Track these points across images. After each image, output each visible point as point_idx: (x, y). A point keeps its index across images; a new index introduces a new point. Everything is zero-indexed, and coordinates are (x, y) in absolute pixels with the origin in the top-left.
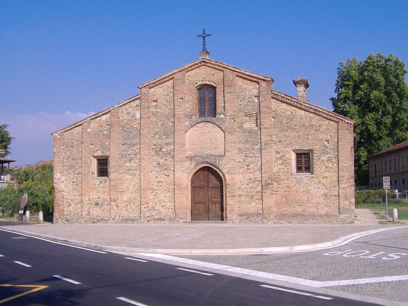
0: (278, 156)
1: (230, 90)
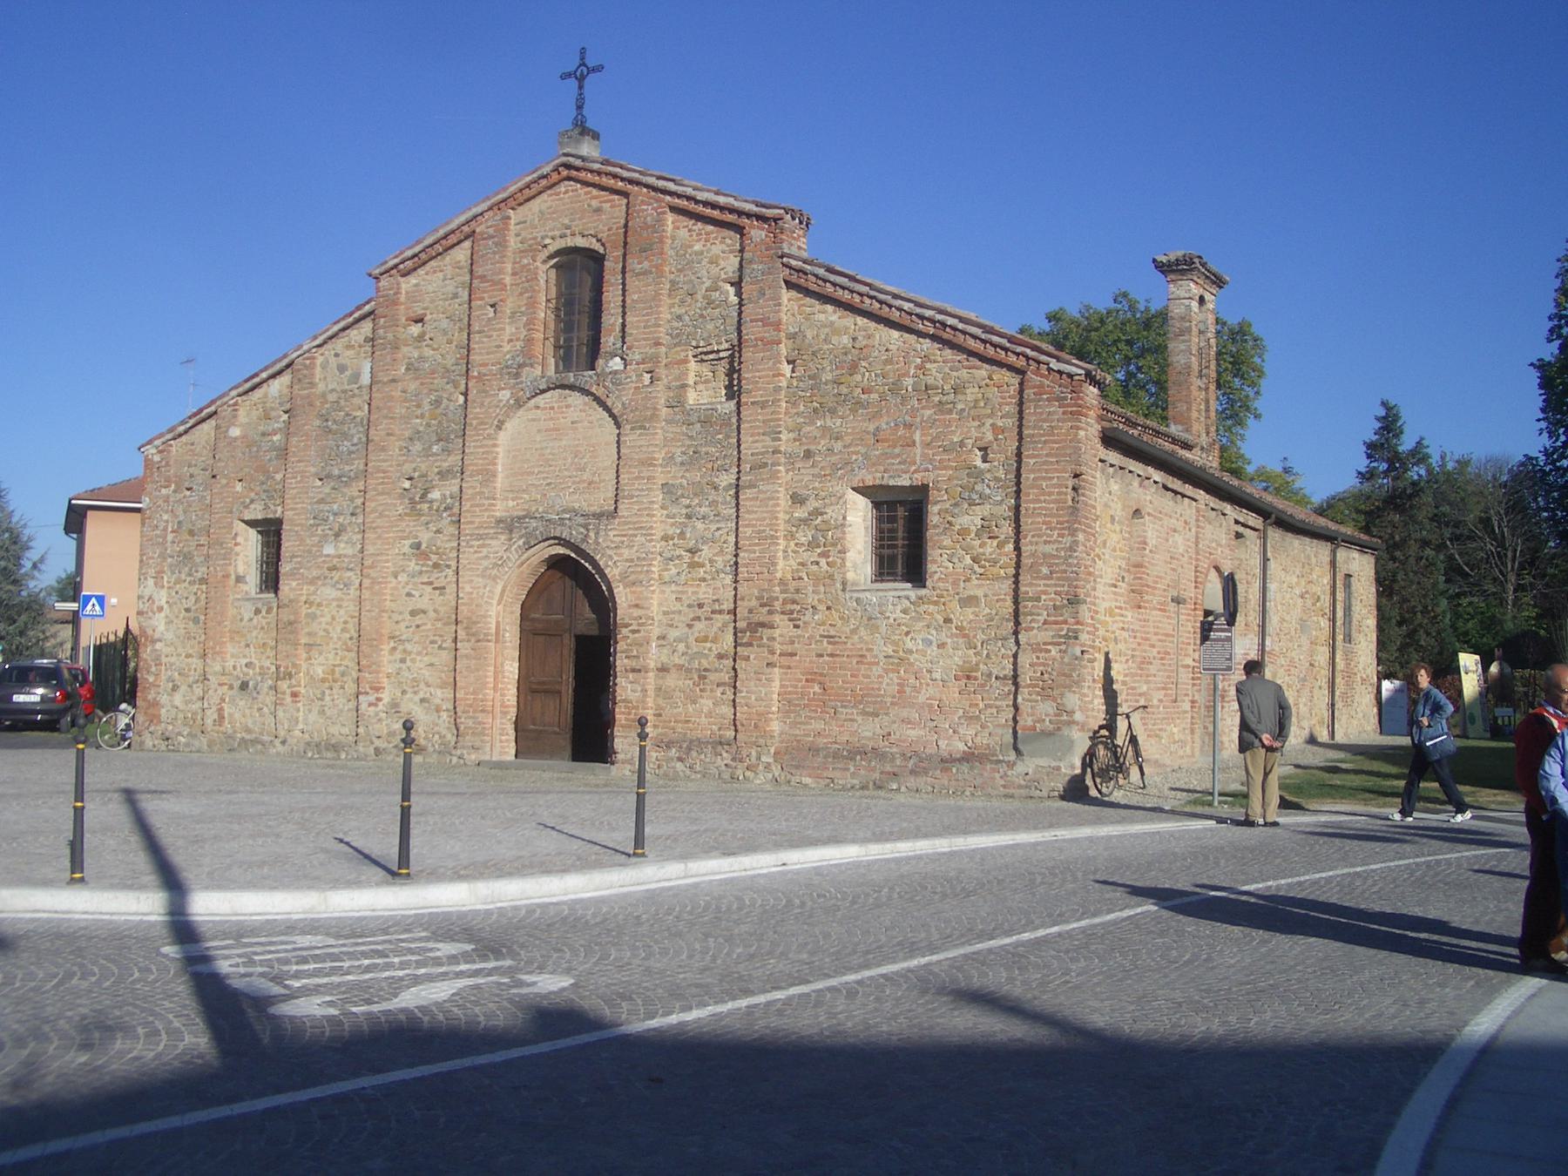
0: (800, 513)
1: (646, 264)
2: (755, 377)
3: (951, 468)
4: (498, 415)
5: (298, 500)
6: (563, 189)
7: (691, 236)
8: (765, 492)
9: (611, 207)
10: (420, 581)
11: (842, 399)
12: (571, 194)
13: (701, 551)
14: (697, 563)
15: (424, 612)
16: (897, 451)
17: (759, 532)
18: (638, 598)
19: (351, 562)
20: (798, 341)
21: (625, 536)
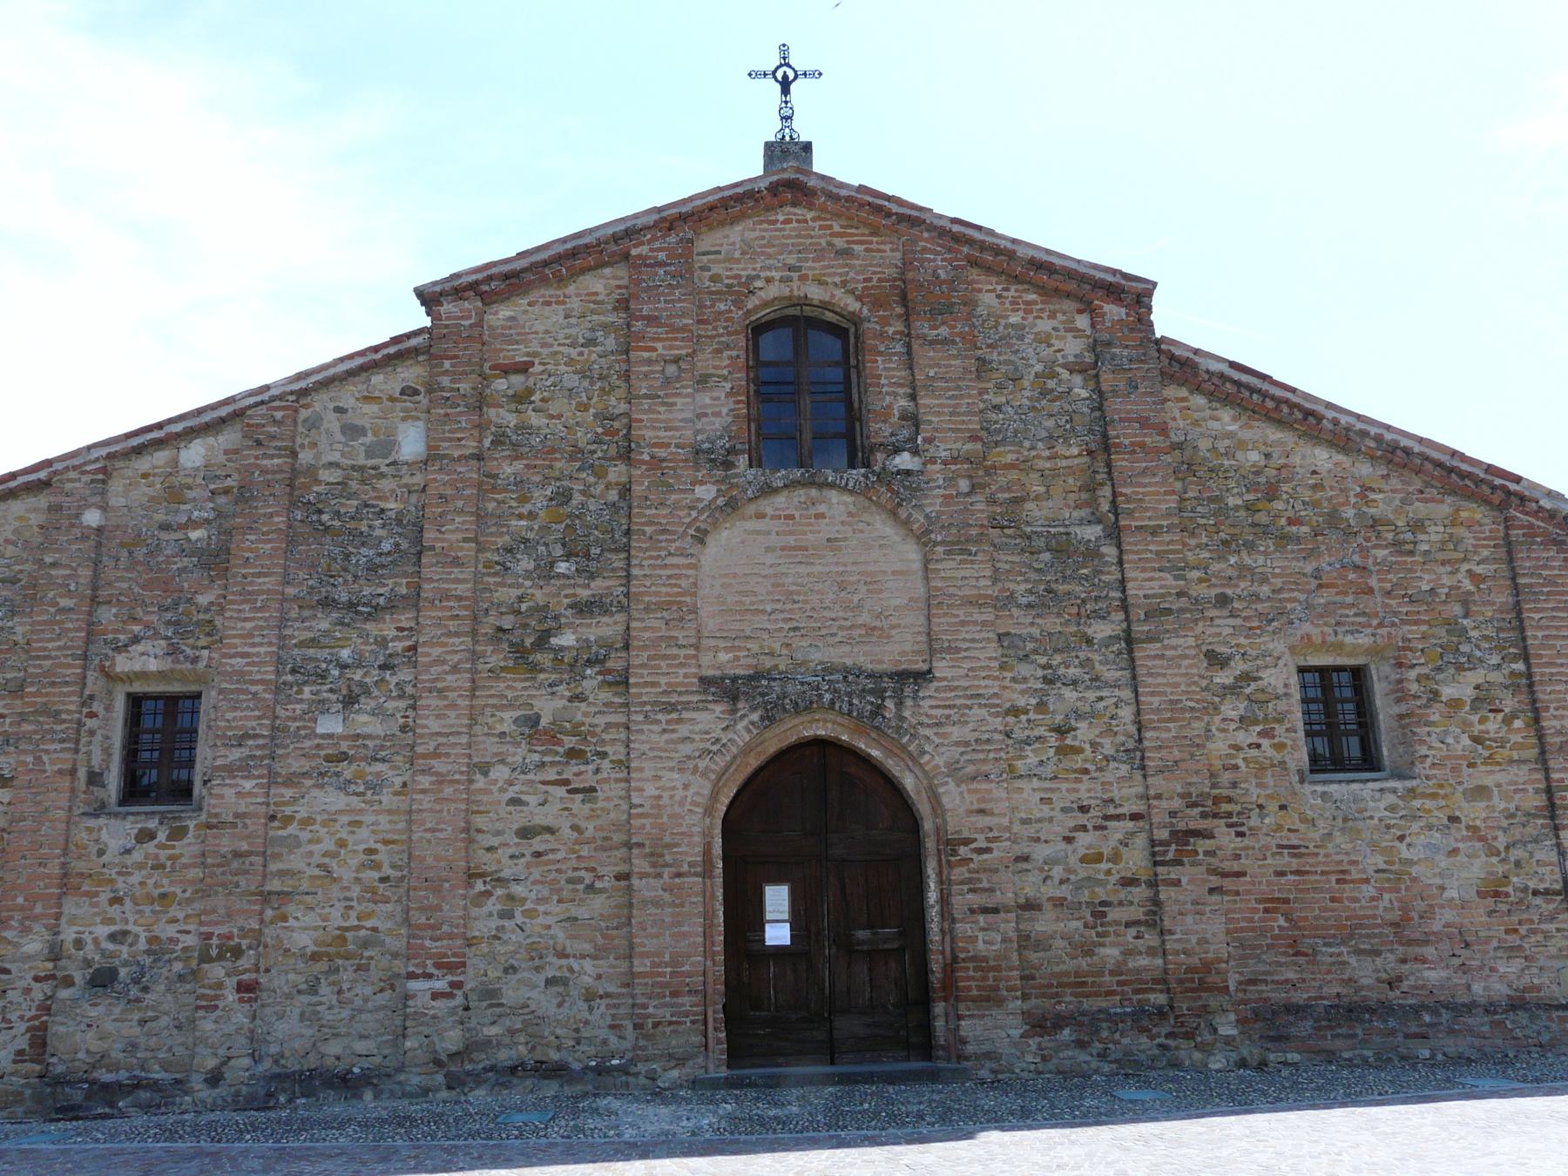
0: (1223, 678)
1: (944, 331)
2: (1138, 493)
3: (1424, 622)
4: (695, 519)
5: (258, 640)
6: (781, 218)
7: (1003, 303)
8: (1175, 648)
9: (866, 250)
10: (539, 777)
11: (1263, 531)
12: (795, 225)
13: (1075, 729)
14: (1072, 747)
15: (550, 830)
16: (1350, 599)
17: (1172, 702)
18: (983, 800)
19: (382, 748)
20: (1189, 452)
21: (949, 707)
